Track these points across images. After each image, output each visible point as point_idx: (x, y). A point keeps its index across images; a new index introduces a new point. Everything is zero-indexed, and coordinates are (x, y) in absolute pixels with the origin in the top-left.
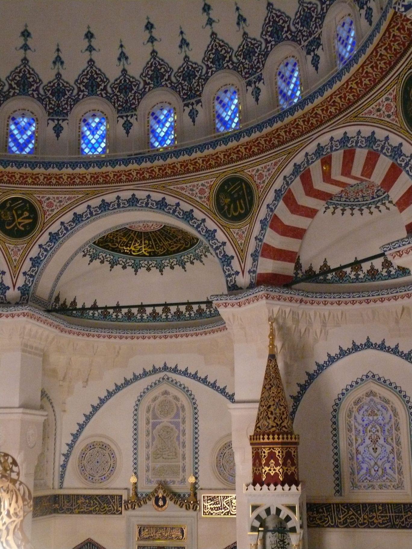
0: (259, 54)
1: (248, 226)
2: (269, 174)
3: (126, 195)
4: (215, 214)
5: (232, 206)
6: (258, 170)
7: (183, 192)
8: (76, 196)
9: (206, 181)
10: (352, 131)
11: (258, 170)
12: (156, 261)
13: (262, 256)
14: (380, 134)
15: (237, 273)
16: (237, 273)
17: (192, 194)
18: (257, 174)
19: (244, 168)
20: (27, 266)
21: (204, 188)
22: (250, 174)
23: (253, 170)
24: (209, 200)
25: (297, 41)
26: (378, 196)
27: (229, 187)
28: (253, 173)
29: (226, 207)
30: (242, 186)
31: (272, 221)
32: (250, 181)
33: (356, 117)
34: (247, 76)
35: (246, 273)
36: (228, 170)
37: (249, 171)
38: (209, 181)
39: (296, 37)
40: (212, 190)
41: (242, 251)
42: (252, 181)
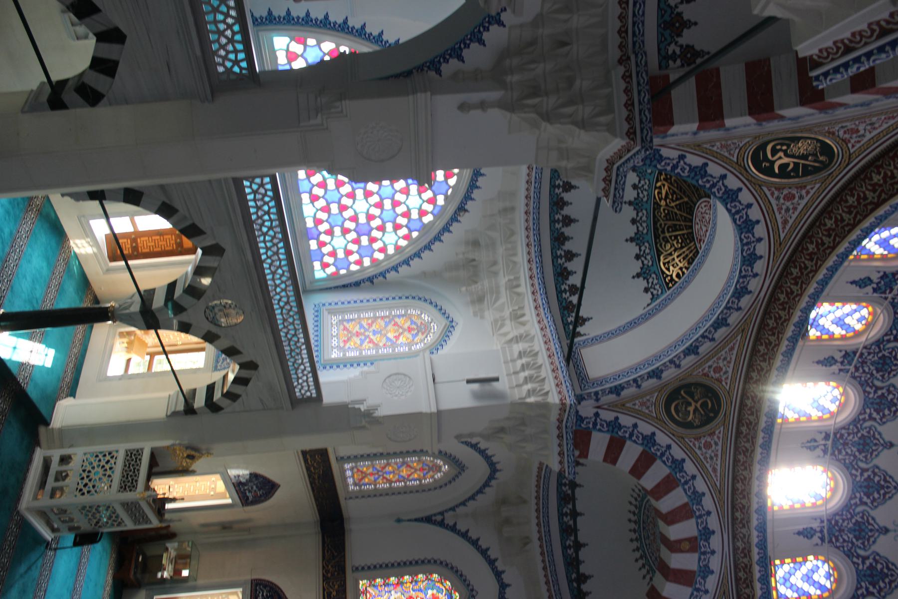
2: (706, 458)
3: (754, 285)
6: (716, 444)
7: (727, 349)
8: (786, 231)
11: (716, 444)
12: (647, 202)
15: (597, 400)
16: (597, 400)
17: (719, 359)
18: (712, 442)
20: (695, 160)
23: (719, 438)
26: (644, 528)
34: (838, 436)
35: (595, 410)
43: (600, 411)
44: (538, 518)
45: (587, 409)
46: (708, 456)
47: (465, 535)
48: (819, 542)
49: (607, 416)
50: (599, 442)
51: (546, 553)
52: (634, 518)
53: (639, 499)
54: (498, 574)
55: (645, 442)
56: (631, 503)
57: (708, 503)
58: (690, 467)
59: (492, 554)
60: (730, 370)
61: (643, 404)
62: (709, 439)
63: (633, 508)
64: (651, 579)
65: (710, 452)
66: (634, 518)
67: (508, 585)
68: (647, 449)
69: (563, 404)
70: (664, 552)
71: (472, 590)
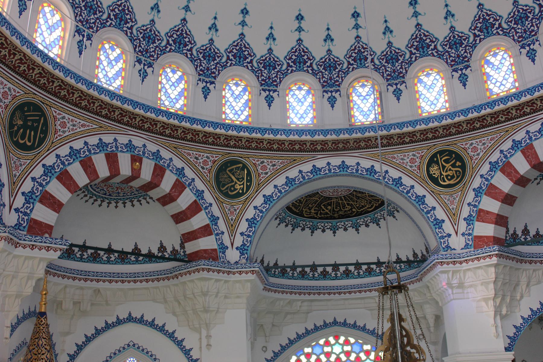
0: (97, 18)
1: (29, 161)
2: (72, 129)
4: (5, 127)
5: (22, 130)
6: (64, 118)
9: (14, 88)
10: (165, 154)
13: (41, 201)
14: (189, 173)
16: (4, 205)
18: (62, 121)
19: (53, 105)
21: (9, 93)
22: (55, 114)
24: (6, 108)
25: (134, 44)
26: (110, 195)
27: (29, 111)
28: (58, 117)
29: (16, 128)
30: (40, 119)
31: (61, 174)
32: (50, 121)
33: (175, 148)
35: (12, 210)
36: (39, 96)
37: (56, 112)
38: (17, 90)
39: (134, 40)
40: (14, 101)
41: (14, 183)
42: (53, 123)
43: (14, 207)
44: (80, 280)
45: (11, 219)
46: (71, 127)
47: (80, 348)
48: (151, 69)
49: (20, 201)
50: (42, 213)
51: (112, 278)
52: (99, 202)
53: (86, 193)
54: (119, 322)
55: (49, 174)
56: (86, 201)
57: (108, 139)
58: (78, 145)
59: (101, 325)
60: (9, 85)
61: (17, 168)
62: (59, 122)
63: (92, 200)
64: (151, 198)
65: (68, 125)
66: (99, 202)
67: (130, 314)
68: (56, 175)
69: (5, 240)
70: (136, 184)
71: (129, 345)
